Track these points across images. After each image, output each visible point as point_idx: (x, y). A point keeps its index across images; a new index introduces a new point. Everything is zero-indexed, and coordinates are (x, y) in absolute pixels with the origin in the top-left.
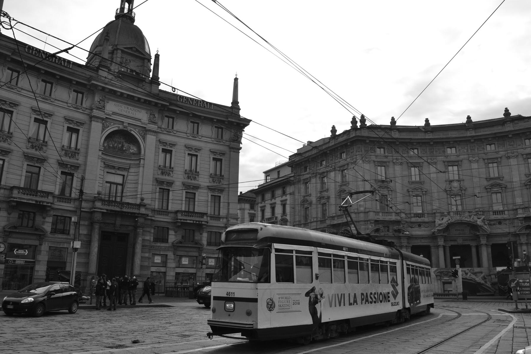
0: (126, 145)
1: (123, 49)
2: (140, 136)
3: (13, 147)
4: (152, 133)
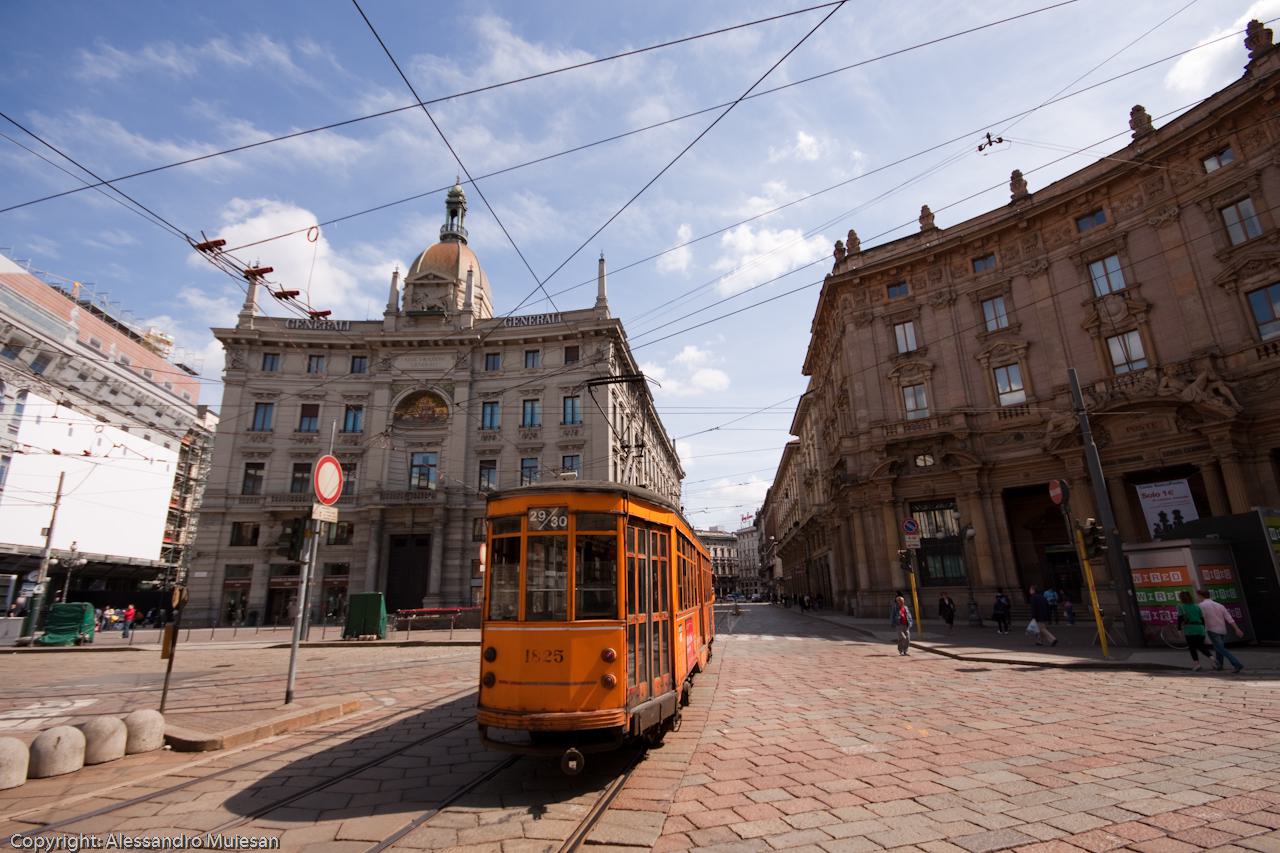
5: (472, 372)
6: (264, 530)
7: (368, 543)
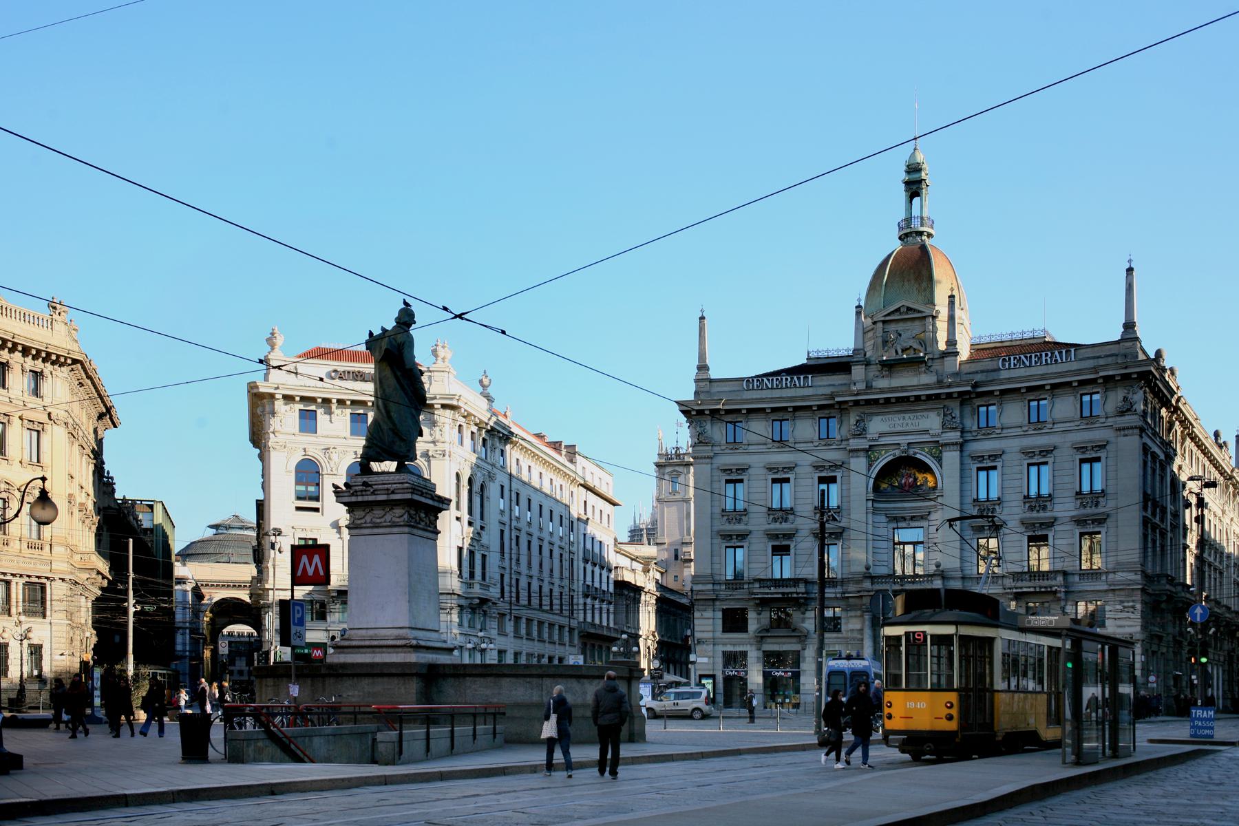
0: (920, 477)
1: (883, 319)
2: (932, 459)
3: (750, 528)
4: (952, 447)
5: (962, 432)
6: (752, 616)
7: (861, 631)
